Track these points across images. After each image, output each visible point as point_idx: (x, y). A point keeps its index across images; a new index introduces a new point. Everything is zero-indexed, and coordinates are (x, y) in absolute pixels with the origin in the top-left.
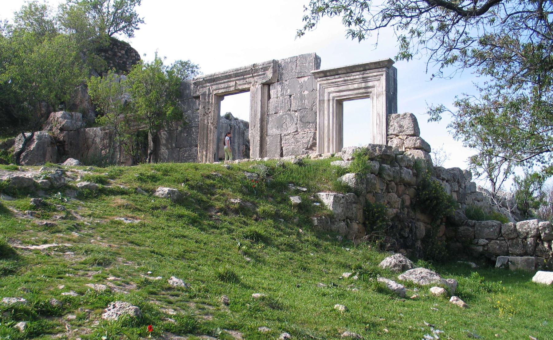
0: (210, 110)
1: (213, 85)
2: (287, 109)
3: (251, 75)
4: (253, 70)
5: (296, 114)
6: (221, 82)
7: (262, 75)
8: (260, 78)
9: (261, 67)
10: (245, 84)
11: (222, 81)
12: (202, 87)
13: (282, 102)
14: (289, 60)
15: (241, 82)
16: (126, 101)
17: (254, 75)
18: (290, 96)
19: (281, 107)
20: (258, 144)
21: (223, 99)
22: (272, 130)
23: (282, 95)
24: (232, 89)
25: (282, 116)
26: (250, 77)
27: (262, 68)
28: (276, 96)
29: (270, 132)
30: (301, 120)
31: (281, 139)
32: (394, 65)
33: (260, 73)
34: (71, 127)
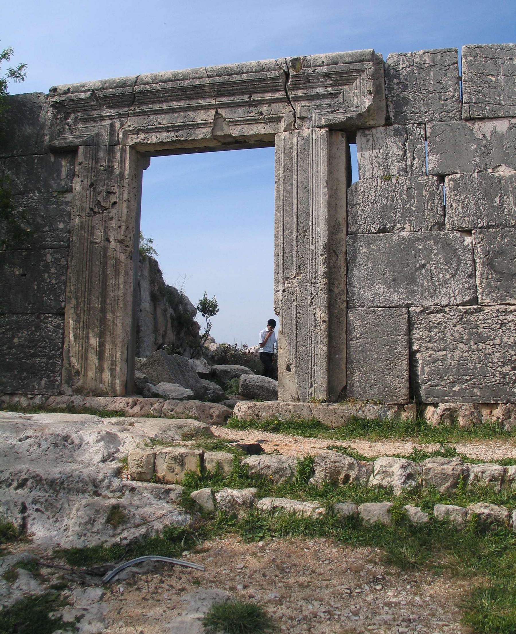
0: (113, 198)
1: (127, 116)
2: (432, 221)
3: (281, 94)
4: (293, 80)
5: (468, 240)
6: (158, 107)
7: (325, 96)
8: (318, 107)
9: (324, 69)
10: (256, 121)
11: (165, 106)
12: (86, 120)
13: (410, 196)
14: (427, 59)
15: (240, 113)
17: (292, 94)
18: (441, 178)
19: (406, 214)
20: (321, 333)
22: (371, 289)
23: (404, 171)
24: (202, 133)
25: (410, 244)
26: (278, 100)
27: (327, 75)
28: (379, 171)
29: (362, 293)
30: (490, 265)
31: (410, 325)
33: (320, 90)
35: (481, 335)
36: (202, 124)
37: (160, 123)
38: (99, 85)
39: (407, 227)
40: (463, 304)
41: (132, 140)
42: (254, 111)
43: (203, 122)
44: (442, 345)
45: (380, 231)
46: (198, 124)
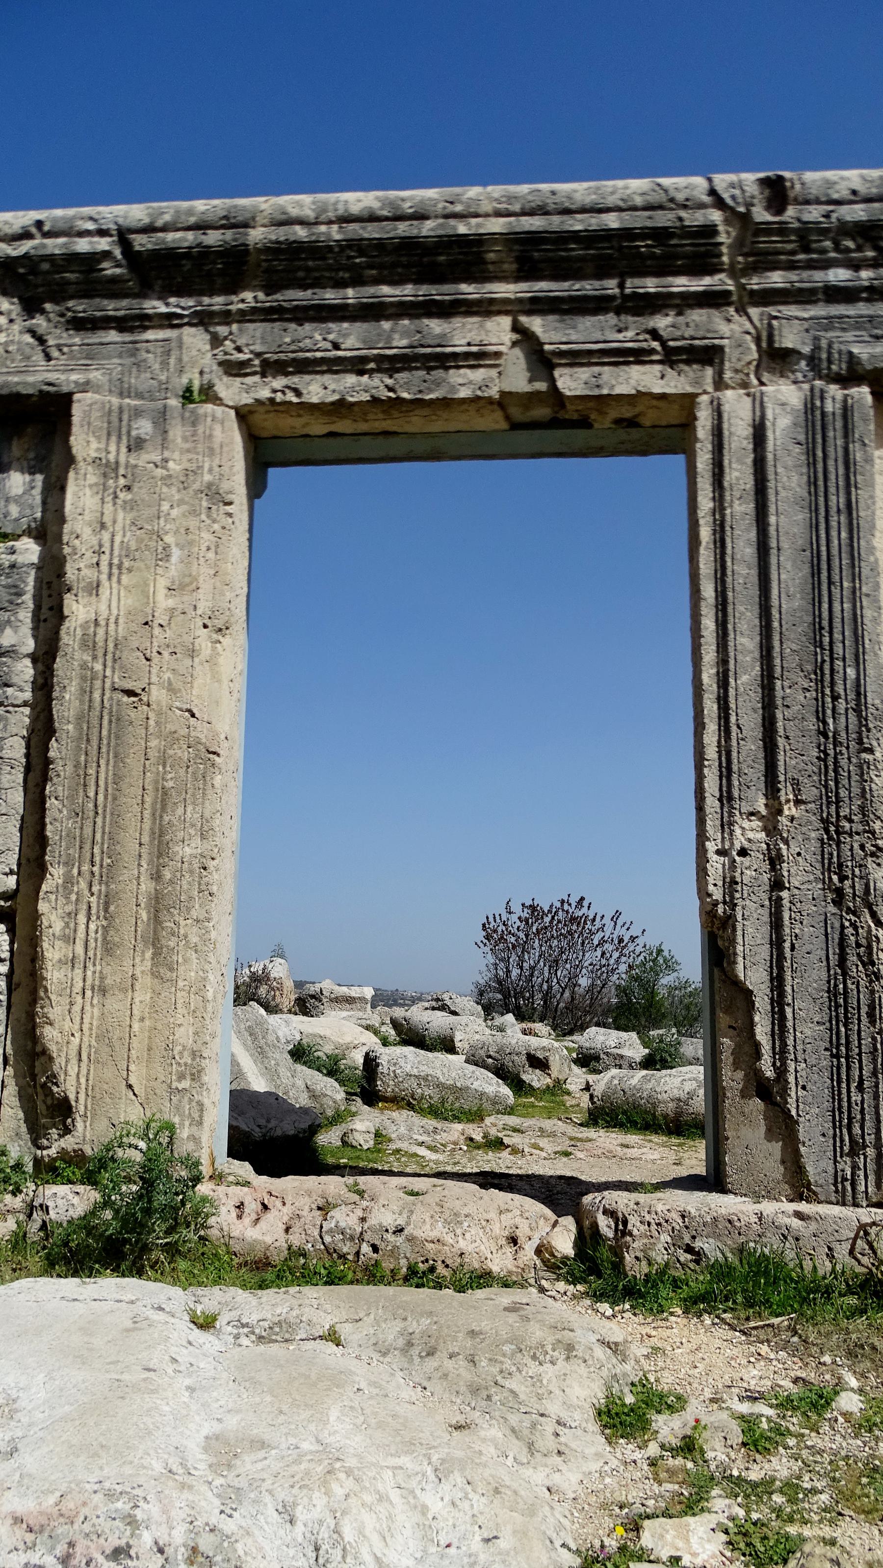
1: (226, 317)
6: (330, 296)
10: (638, 356)
15: (589, 331)
33: (839, 275)
36: (467, 355)
37: (336, 346)
43: (474, 349)
46: (455, 356)
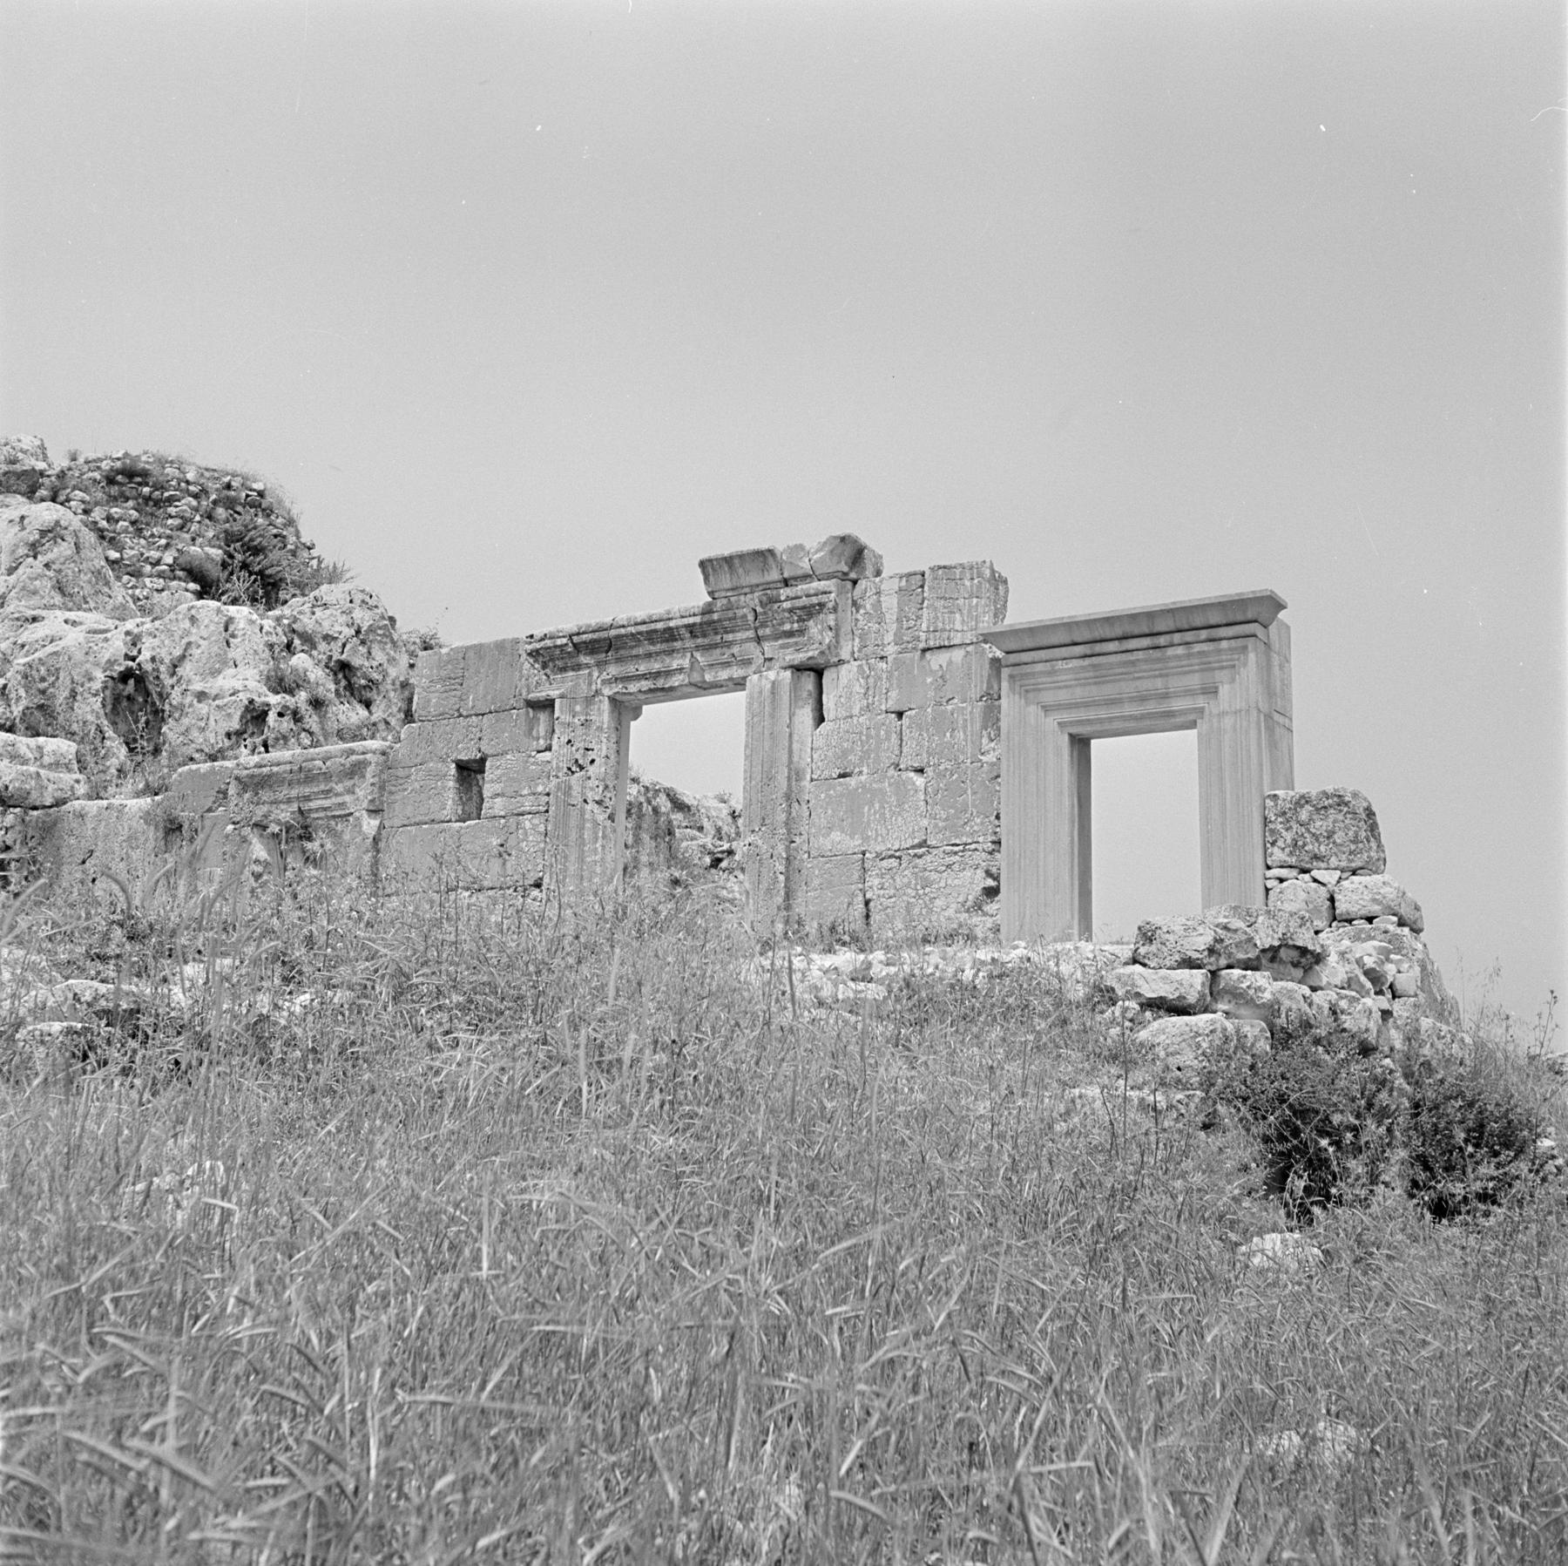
0: (591, 755)
3: (751, 634)
10: (727, 664)
13: (868, 736)
16: (251, 702)
18: (900, 715)
21: (636, 712)
32: (1282, 615)
34: (34, 794)
35: (926, 879)
38: (575, 630)
39: (865, 770)
40: (913, 847)
41: (607, 691)
42: (728, 652)
44: (892, 892)
45: (842, 776)
